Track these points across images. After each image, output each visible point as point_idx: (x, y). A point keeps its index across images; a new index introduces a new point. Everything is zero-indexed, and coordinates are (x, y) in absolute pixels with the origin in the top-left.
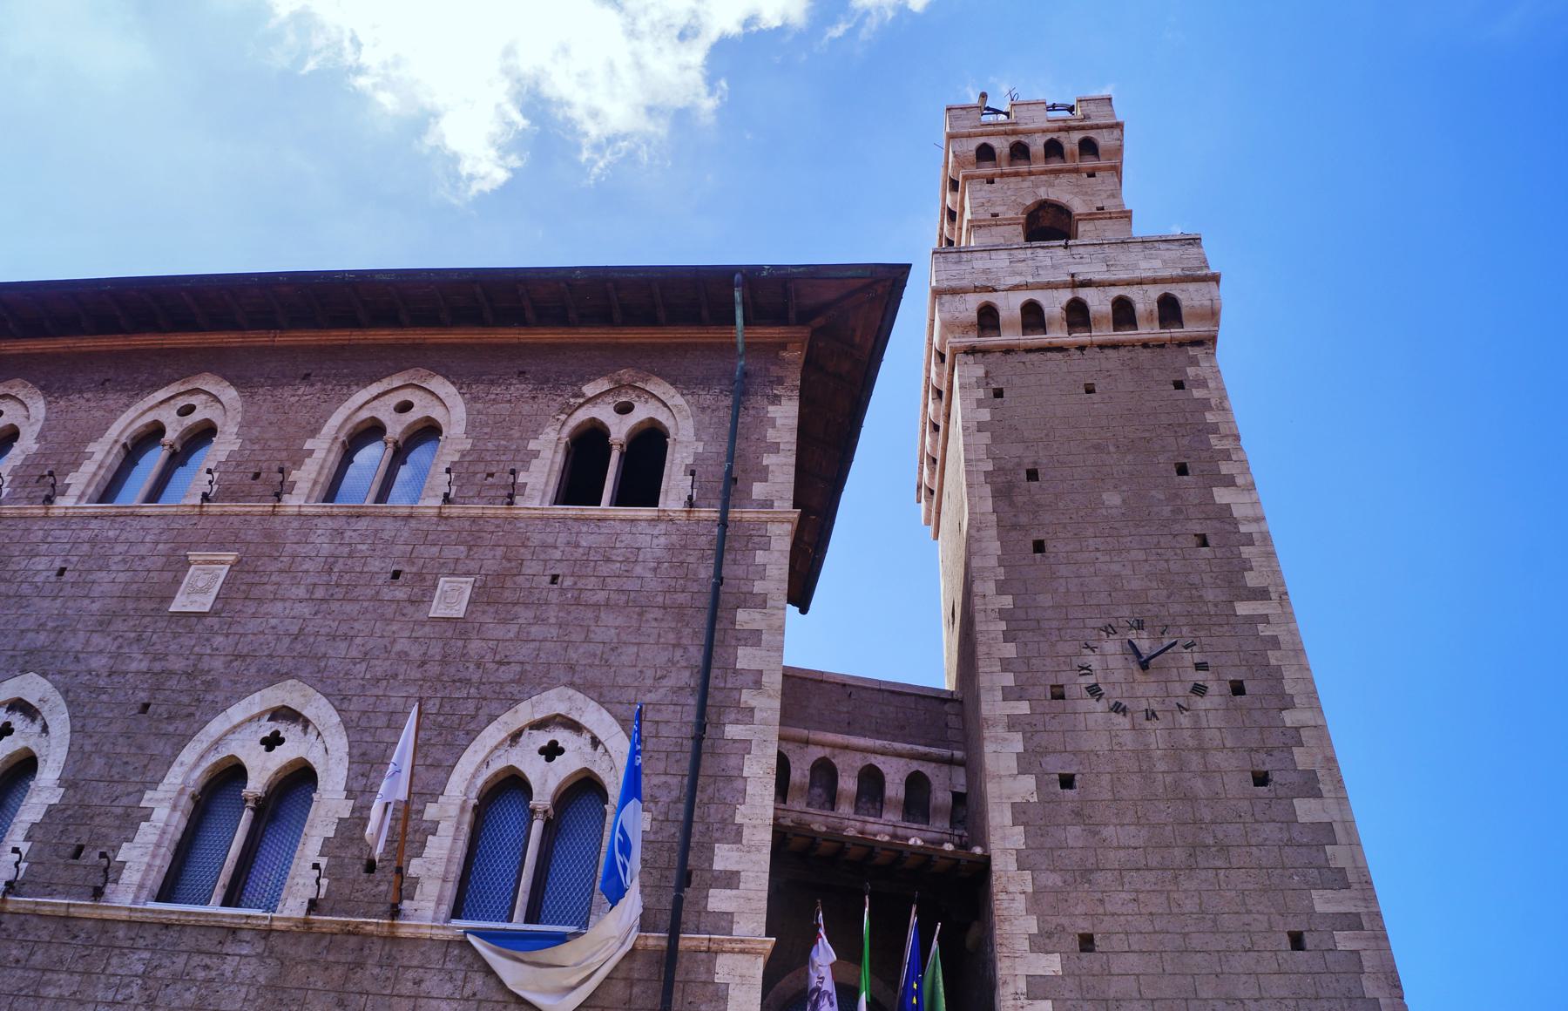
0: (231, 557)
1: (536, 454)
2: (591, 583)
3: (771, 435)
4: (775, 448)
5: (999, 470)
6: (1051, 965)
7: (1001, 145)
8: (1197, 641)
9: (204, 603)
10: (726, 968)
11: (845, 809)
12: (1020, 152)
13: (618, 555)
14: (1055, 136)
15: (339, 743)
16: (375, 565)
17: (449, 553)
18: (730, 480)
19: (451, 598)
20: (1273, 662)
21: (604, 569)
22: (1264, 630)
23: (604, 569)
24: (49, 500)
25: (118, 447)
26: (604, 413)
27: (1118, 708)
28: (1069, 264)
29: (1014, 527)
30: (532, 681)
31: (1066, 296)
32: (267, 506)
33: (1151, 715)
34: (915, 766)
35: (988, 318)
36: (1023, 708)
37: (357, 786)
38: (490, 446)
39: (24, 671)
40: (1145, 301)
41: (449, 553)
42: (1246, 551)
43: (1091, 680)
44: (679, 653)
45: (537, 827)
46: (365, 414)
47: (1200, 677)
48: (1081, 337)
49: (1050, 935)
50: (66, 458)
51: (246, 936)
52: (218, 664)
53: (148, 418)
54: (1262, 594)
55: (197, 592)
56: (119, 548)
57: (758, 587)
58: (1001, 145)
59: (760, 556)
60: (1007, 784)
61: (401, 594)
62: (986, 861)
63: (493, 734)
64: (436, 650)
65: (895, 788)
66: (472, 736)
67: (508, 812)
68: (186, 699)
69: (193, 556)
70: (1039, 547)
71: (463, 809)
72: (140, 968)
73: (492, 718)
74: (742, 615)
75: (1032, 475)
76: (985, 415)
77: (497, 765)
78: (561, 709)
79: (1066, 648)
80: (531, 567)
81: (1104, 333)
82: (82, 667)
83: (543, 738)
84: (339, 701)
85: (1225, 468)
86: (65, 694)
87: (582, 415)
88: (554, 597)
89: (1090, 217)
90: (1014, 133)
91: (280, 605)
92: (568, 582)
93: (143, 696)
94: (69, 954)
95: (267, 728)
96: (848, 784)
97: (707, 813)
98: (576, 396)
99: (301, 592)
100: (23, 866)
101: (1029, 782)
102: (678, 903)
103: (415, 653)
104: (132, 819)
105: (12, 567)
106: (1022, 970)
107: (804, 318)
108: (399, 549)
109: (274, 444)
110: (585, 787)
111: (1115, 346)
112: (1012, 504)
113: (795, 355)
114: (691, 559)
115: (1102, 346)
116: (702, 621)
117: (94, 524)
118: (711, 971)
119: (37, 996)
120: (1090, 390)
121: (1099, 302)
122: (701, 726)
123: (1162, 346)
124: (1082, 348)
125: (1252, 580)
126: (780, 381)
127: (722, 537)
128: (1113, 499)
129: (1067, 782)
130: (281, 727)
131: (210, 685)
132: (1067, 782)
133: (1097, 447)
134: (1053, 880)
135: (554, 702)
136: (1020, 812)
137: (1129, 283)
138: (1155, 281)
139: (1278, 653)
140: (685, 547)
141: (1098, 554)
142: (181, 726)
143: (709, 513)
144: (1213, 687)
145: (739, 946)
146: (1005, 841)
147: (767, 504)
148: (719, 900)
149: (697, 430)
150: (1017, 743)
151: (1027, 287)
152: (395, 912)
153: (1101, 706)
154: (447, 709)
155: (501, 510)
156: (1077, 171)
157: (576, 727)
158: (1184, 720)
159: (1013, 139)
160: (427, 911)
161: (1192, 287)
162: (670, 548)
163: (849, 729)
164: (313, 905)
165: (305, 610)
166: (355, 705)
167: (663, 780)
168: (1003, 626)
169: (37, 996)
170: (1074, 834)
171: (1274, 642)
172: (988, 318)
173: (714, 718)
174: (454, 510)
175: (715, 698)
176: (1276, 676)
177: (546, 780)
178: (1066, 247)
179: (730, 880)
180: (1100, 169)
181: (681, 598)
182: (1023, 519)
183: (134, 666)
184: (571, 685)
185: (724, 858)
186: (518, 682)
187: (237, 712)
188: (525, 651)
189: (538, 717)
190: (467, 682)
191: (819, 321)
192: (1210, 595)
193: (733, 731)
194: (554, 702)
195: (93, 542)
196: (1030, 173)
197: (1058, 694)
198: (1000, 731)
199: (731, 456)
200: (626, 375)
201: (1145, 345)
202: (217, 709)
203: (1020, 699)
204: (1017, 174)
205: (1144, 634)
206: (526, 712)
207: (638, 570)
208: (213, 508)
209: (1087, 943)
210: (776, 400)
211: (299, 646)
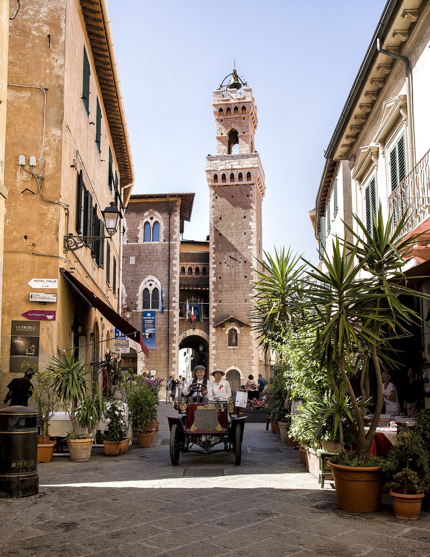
6: (215, 304)
7: (224, 109)
11: (194, 274)
12: (229, 109)
26: (148, 219)
27: (228, 266)
30: (146, 275)
31: (230, 172)
33: (233, 267)
34: (204, 266)
35: (216, 177)
36: (215, 266)
45: (151, 296)
48: (232, 183)
58: (224, 109)
59: (175, 250)
60: (212, 279)
62: (209, 290)
63: (143, 283)
64: (132, 270)
74: (173, 261)
77: (144, 287)
78: (151, 279)
79: (223, 255)
81: (237, 182)
83: (149, 283)
87: (145, 221)
96: (194, 271)
97: (171, 293)
98: (143, 216)
101: (215, 278)
103: (130, 271)
110: (156, 290)
111: (238, 185)
115: (236, 185)
122: (169, 280)
124: (232, 185)
126: (176, 211)
127: (169, 245)
136: (213, 282)
137: (242, 169)
144: (242, 262)
146: (212, 286)
148: (173, 304)
150: (214, 272)
153: (226, 265)
155: (136, 243)
158: (237, 267)
161: (253, 170)
162: (162, 249)
167: (165, 289)
168: (213, 251)
172: (216, 177)
174: (129, 244)
175: (171, 275)
177: (151, 289)
179: (175, 302)
181: (165, 259)
185: (174, 299)
188: (145, 269)
194: (150, 277)
197: (220, 263)
198: (212, 270)
201: (244, 185)
206: (146, 279)
209: (220, 302)
210: (176, 216)
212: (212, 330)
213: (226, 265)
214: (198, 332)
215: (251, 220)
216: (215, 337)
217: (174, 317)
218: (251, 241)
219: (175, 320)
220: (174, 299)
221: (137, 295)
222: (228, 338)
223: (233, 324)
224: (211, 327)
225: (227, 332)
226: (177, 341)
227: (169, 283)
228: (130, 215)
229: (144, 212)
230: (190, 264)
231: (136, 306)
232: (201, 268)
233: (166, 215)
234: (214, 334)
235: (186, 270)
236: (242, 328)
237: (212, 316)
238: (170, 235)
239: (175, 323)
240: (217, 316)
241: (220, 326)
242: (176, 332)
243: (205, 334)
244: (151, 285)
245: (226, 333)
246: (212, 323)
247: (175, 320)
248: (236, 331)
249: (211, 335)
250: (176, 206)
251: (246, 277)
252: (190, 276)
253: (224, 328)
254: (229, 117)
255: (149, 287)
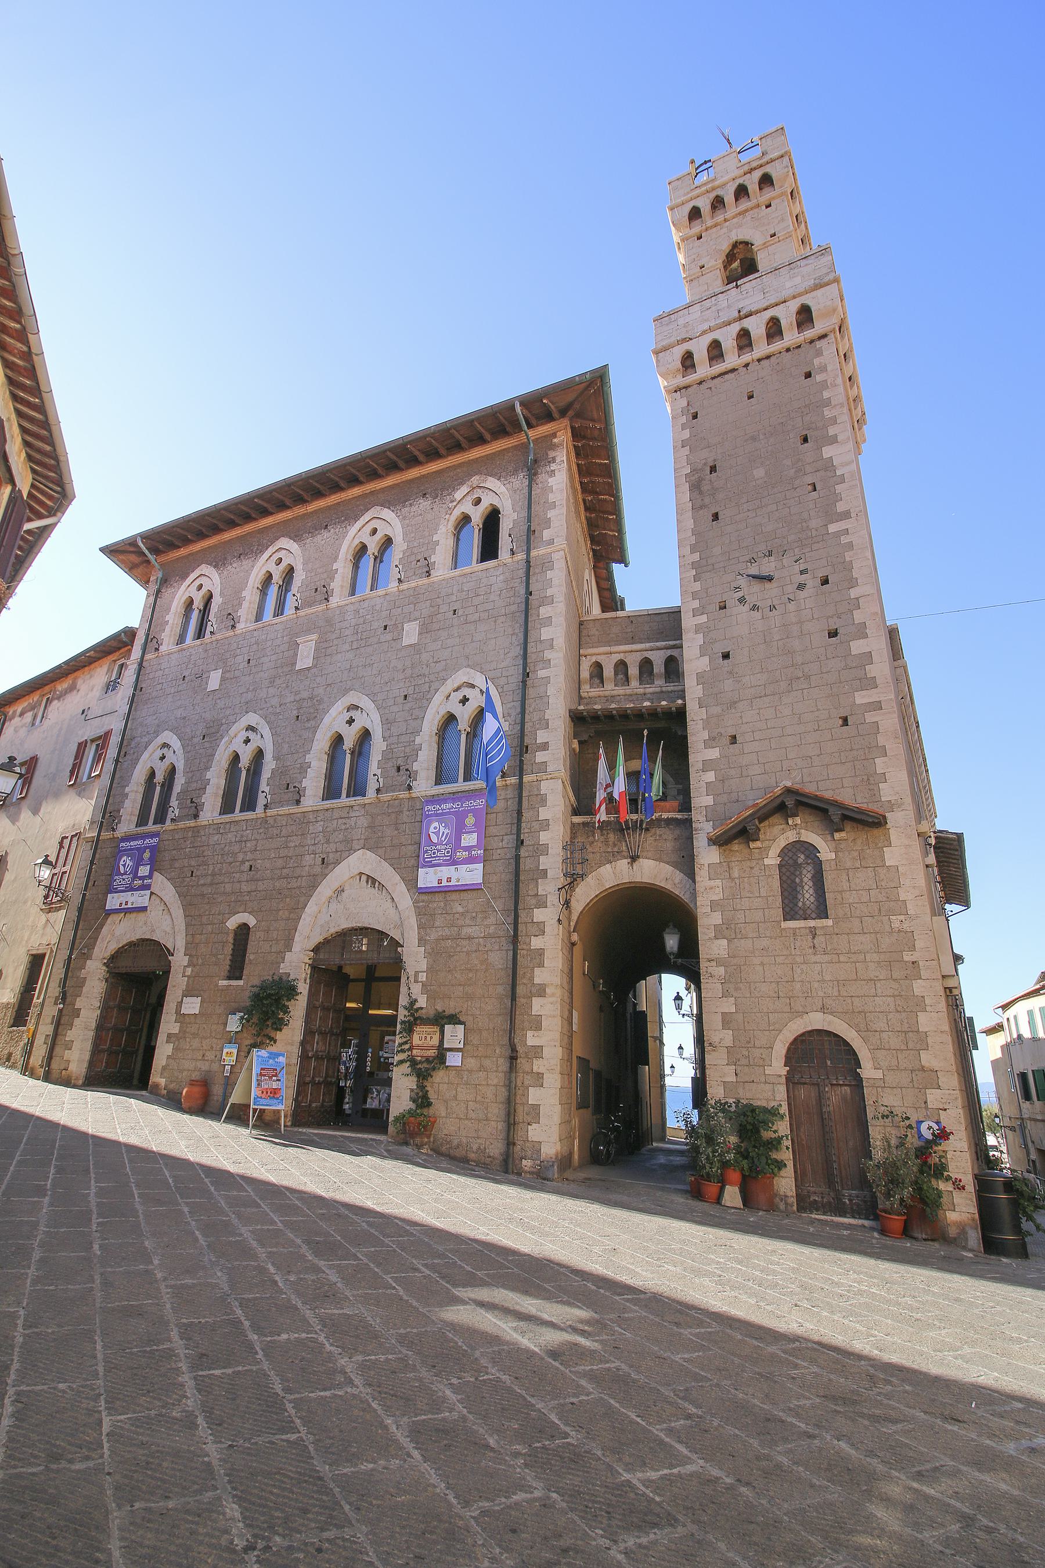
0: (315, 637)
1: (437, 543)
2: (471, 610)
3: (551, 498)
4: (554, 505)
5: (694, 471)
6: (714, 754)
7: (704, 204)
8: (803, 556)
9: (309, 663)
10: (545, 787)
11: (634, 683)
12: (718, 203)
13: (482, 591)
14: (740, 181)
15: (376, 716)
16: (375, 625)
17: (406, 609)
18: (530, 532)
19: (411, 633)
20: (848, 559)
21: (476, 601)
22: (844, 540)
23: (476, 601)
24: (233, 627)
25: (255, 590)
26: (467, 508)
27: (754, 608)
28: (738, 300)
29: (701, 508)
31: (735, 328)
32: (323, 607)
33: (772, 608)
34: (669, 652)
35: (688, 361)
36: (704, 618)
37: (387, 735)
38: (416, 544)
39: (247, 712)
40: (787, 315)
41: (406, 609)
42: (839, 488)
43: (740, 594)
44: (514, 637)
45: (463, 737)
46: (356, 542)
47: (802, 578)
48: (747, 358)
49: (714, 739)
50: (235, 602)
51: (355, 808)
52: (321, 691)
53: (264, 571)
54: (846, 515)
55: (305, 659)
56: (269, 643)
57: (549, 592)
58: (704, 204)
59: (549, 574)
60: (694, 661)
61: (388, 636)
63: (438, 698)
65: (659, 668)
66: (429, 700)
67: (450, 732)
68: (312, 710)
69: (299, 640)
70: (716, 517)
71: (431, 736)
72: (321, 829)
73: (437, 690)
75: (713, 469)
76: (686, 434)
77: (443, 712)
80: (444, 608)
81: (761, 348)
82: (268, 705)
83: (459, 695)
84: (372, 696)
85: (832, 431)
86: (265, 719)
87: (457, 513)
88: (456, 622)
89: (765, 245)
90: (713, 189)
91: (339, 655)
92: (460, 612)
93: (295, 713)
94: (294, 827)
95: (347, 716)
96: (633, 671)
98: (452, 502)
99: (347, 647)
100: (269, 797)
101: (706, 659)
102: (521, 761)
104: (304, 768)
105: (229, 664)
106: (700, 759)
107: (563, 413)
108: (385, 614)
109: (320, 571)
111: (768, 357)
112: (701, 493)
113: (564, 437)
114: (516, 585)
115: (759, 360)
116: (522, 620)
117: (256, 633)
118: (539, 790)
119: (287, 847)
120: (750, 397)
121: (757, 327)
123: (799, 346)
124: (747, 365)
125: (841, 507)
128: (759, 473)
129: (726, 656)
130: (354, 714)
131: (320, 702)
132: (726, 656)
133: (754, 439)
134: (716, 710)
135: (461, 676)
136: (700, 677)
138: (794, 297)
139: (851, 553)
140: (513, 579)
141: (749, 513)
142: (312, 723)
143: (521, 556)
144: (810, 584)
145: (549, 777)
147: (551, 542)
148: (540, 757)
149: (513, 505)
150: (700, 639)
151: (711, 330)
152: (410, 788)
153: (747, 607)
154: (417, 690)
156: (758, 206)
157: (473, 686)
158: (791, 607)
159: (712, 195)
160: (424, 785)
161: (819, 293)
162: (506, 581)
163: (633, 640)
164: (378, 790)
165: (350, 655)
166: (380, 697)
169: (287, 847)
170: (728, 684)
171: (850, 546)
173: (532, 668)
174: (404, 586)
176: (849, 567)
177: (465, 715)
178: (737, 286)
179: (545, 747)
180: (774, 198)
181: (514, 608)
182: (707, 501)
183: (288, 700)
184: (468, 666)
186: (445, 670)
187: (333, 712)
189: (456, 686)
190: (424, 675)
191: (571, 413)
192: (814, 523)
193: (542, 673)
194: (461, 676)
195: (257, 643)
196: (726, 220)
199: (529, 520)
200: (475, 480)
201: (788, 350)
202: (326, 711)
203: (702, 614)
204: (715, 226)
205: (772, 558)
207: (492, 597)
208: (301, 613)
209: (734, 739)
211: (351, 674)
212: (707, 856)
213: (747, 607)
214: (652, 871)
215: (834, 440)
216: (718, 882)
217: (543, 801)
218: (841, 507)
219: (544, 814)
220: (542, 737)
221: (418, 740)
222: (776, 884)
223: (798, 820)
224: (700, 842)
225: (772, 859)
226: (554, 900)
227: (524, 682)
228: (413, 509)
229: (454, 490)
230: (620, 651)
231: (411, 775)
232: (658, 659)
233: (520, 481)
234: (714, 872)
235: (608, 672)
236: (843, 834)
237: (701, 800)
238: (530, 532)
239: (545, 825)
240: (724, 798)
241: (739, 834)
242: (553, 862)
243: (679, 876)
244: (464, 700)
245: (767, 861)
246: (704, 829)
247: (544, 814)
248: (810, 850)
249: (702, 876)
250: (553, 447)
251: (833, 634)
252: (620, 691)
253: (758, 844)
254: (720, 218)
255: (457, 710)
